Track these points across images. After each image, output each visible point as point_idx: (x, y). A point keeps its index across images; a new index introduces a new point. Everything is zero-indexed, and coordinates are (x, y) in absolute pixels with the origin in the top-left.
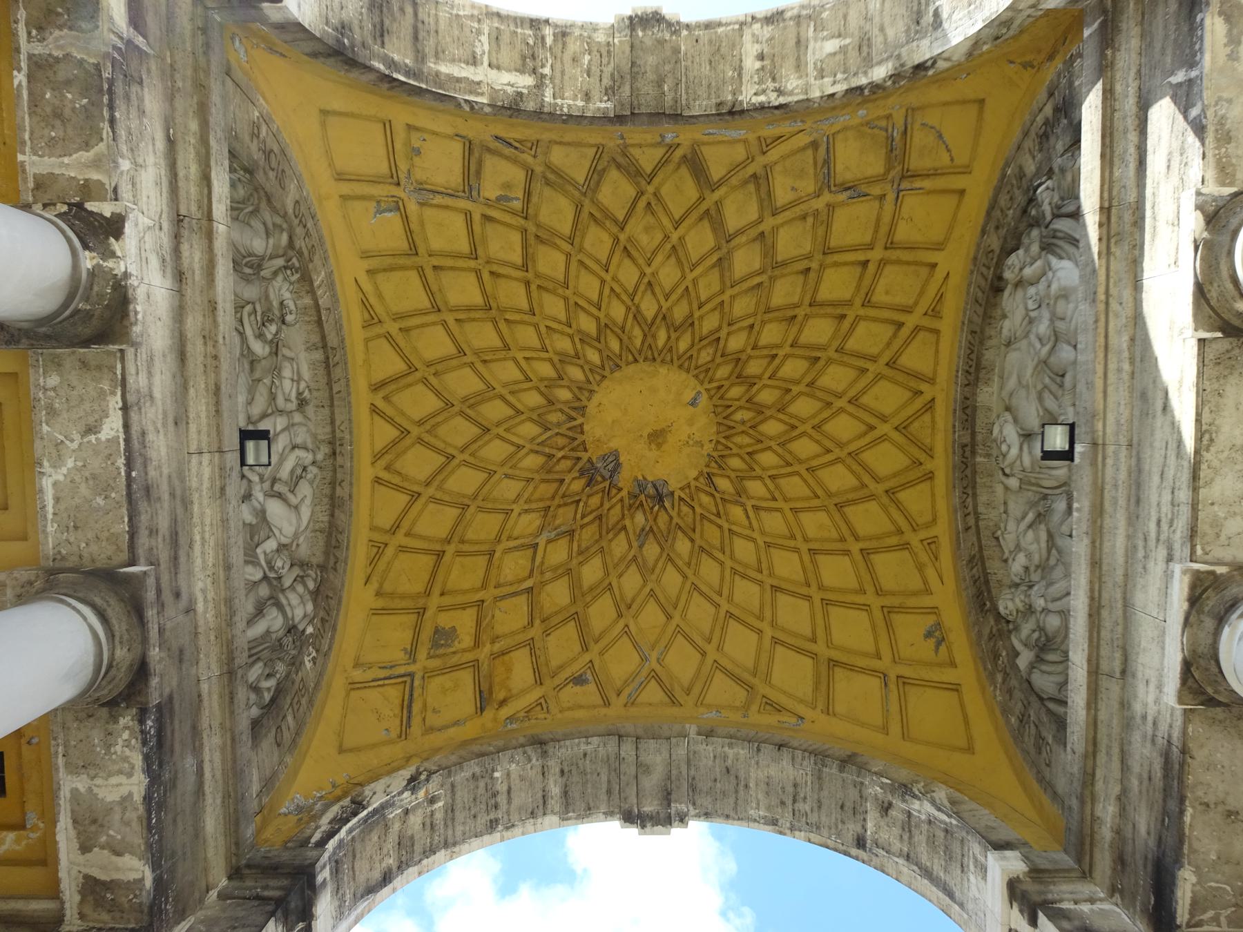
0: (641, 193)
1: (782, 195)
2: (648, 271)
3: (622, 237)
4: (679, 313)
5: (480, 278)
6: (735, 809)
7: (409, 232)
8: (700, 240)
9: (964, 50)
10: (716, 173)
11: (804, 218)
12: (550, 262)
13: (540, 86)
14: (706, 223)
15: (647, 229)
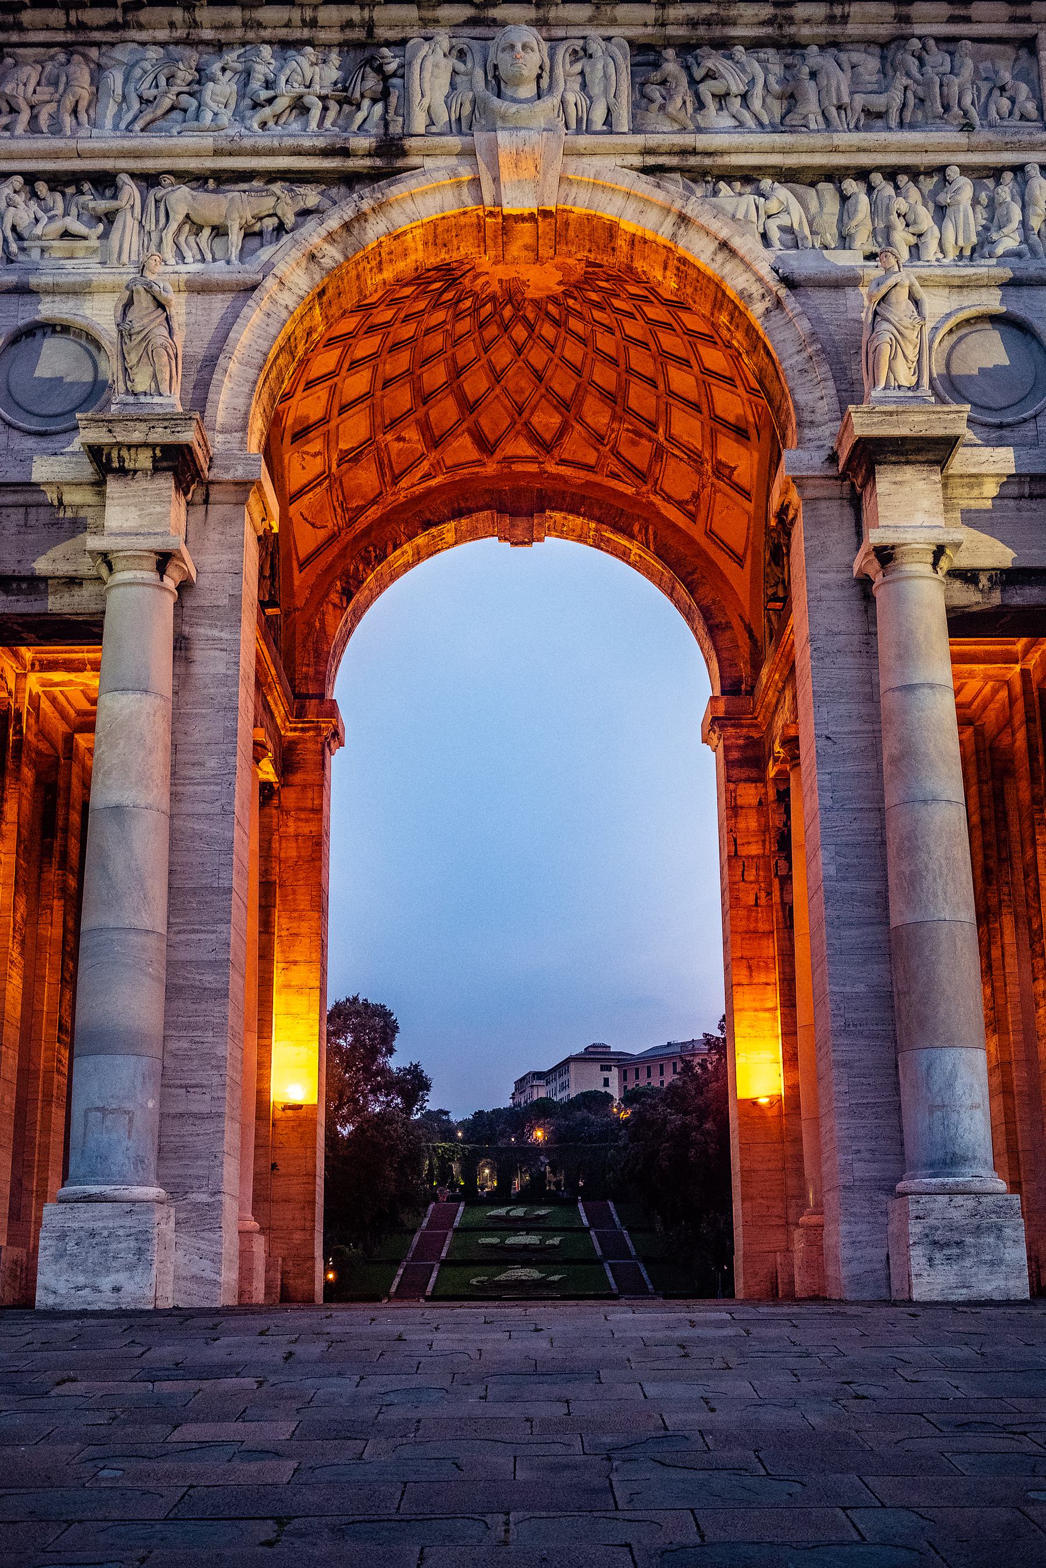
0: (525, 424)
1: (412, 434)
2: (520, 364)
3: (543, 391)
4: (492, 331)
5: (667, 385)
6: (436, 226)
7: (714, 446)
8: (475, 384)
9: (329, 619)
10: (466, 440)
11: (394, 423)
12: (605, 376)
13: (596, 530)
14: (472, 399)
15: (522, 391)
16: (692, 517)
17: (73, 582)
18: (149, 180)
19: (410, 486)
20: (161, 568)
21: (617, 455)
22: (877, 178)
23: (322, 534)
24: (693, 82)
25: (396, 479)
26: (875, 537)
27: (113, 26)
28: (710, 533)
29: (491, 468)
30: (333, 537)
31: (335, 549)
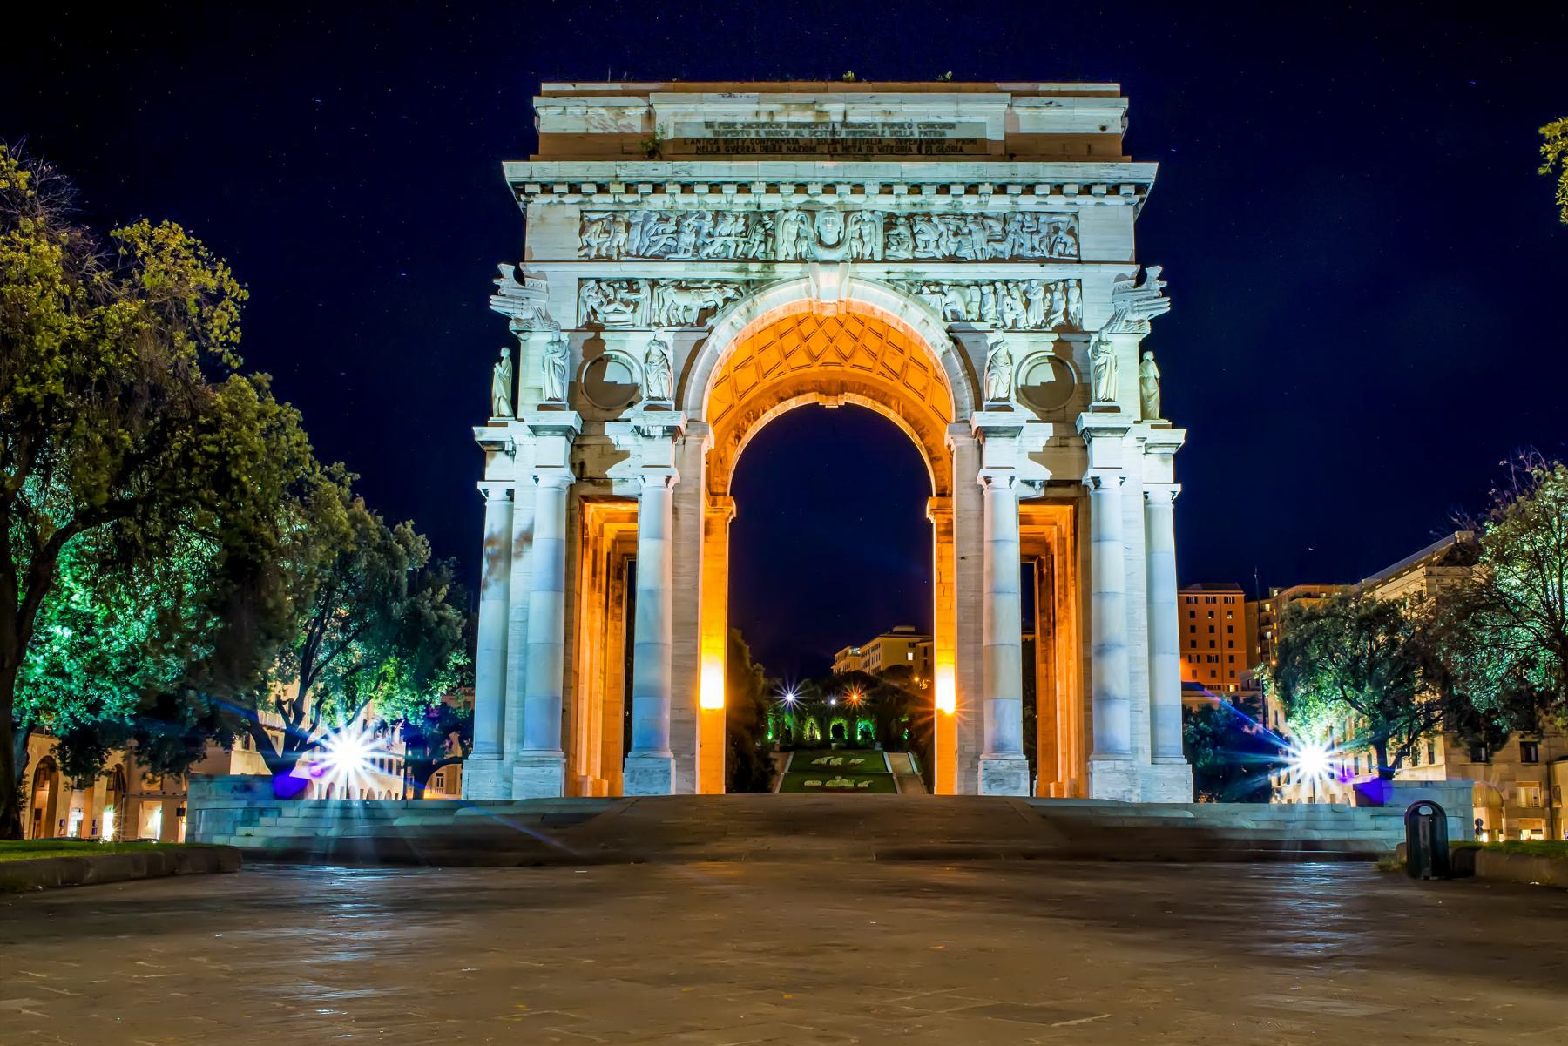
16: (923, 397)
17: (624, 480)
18: (654, 283)
19: (772, 379)
20: (667, 481)
21: (883, 364)
22: (998, 285)
23: (725, 406)
24: (913, 235)
25: (765, 376)
26: (983, 473)
27: (636, 203)
28: (933, 407)
29: (816, 368)
30: (731, 407)
31: (733, 411)
